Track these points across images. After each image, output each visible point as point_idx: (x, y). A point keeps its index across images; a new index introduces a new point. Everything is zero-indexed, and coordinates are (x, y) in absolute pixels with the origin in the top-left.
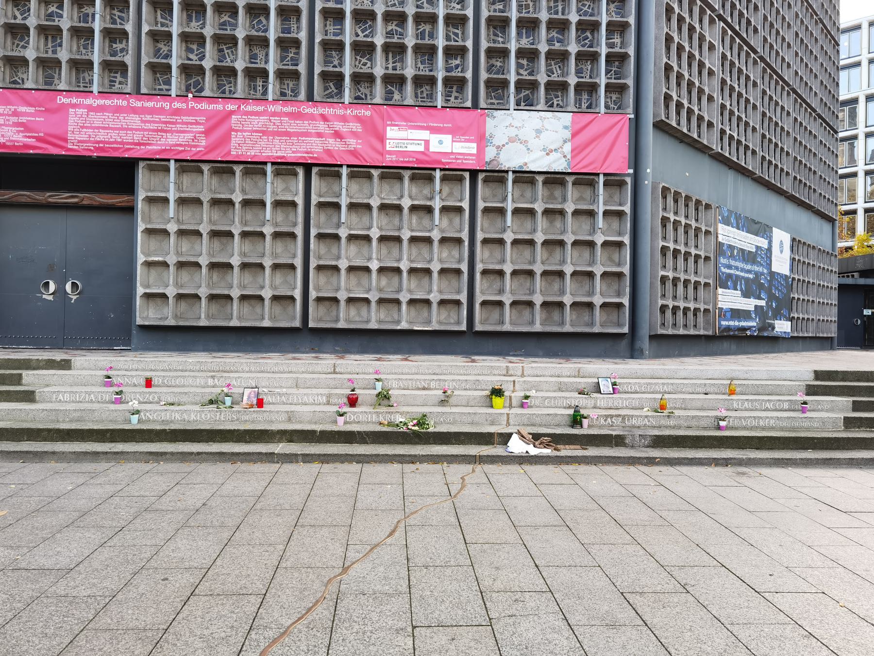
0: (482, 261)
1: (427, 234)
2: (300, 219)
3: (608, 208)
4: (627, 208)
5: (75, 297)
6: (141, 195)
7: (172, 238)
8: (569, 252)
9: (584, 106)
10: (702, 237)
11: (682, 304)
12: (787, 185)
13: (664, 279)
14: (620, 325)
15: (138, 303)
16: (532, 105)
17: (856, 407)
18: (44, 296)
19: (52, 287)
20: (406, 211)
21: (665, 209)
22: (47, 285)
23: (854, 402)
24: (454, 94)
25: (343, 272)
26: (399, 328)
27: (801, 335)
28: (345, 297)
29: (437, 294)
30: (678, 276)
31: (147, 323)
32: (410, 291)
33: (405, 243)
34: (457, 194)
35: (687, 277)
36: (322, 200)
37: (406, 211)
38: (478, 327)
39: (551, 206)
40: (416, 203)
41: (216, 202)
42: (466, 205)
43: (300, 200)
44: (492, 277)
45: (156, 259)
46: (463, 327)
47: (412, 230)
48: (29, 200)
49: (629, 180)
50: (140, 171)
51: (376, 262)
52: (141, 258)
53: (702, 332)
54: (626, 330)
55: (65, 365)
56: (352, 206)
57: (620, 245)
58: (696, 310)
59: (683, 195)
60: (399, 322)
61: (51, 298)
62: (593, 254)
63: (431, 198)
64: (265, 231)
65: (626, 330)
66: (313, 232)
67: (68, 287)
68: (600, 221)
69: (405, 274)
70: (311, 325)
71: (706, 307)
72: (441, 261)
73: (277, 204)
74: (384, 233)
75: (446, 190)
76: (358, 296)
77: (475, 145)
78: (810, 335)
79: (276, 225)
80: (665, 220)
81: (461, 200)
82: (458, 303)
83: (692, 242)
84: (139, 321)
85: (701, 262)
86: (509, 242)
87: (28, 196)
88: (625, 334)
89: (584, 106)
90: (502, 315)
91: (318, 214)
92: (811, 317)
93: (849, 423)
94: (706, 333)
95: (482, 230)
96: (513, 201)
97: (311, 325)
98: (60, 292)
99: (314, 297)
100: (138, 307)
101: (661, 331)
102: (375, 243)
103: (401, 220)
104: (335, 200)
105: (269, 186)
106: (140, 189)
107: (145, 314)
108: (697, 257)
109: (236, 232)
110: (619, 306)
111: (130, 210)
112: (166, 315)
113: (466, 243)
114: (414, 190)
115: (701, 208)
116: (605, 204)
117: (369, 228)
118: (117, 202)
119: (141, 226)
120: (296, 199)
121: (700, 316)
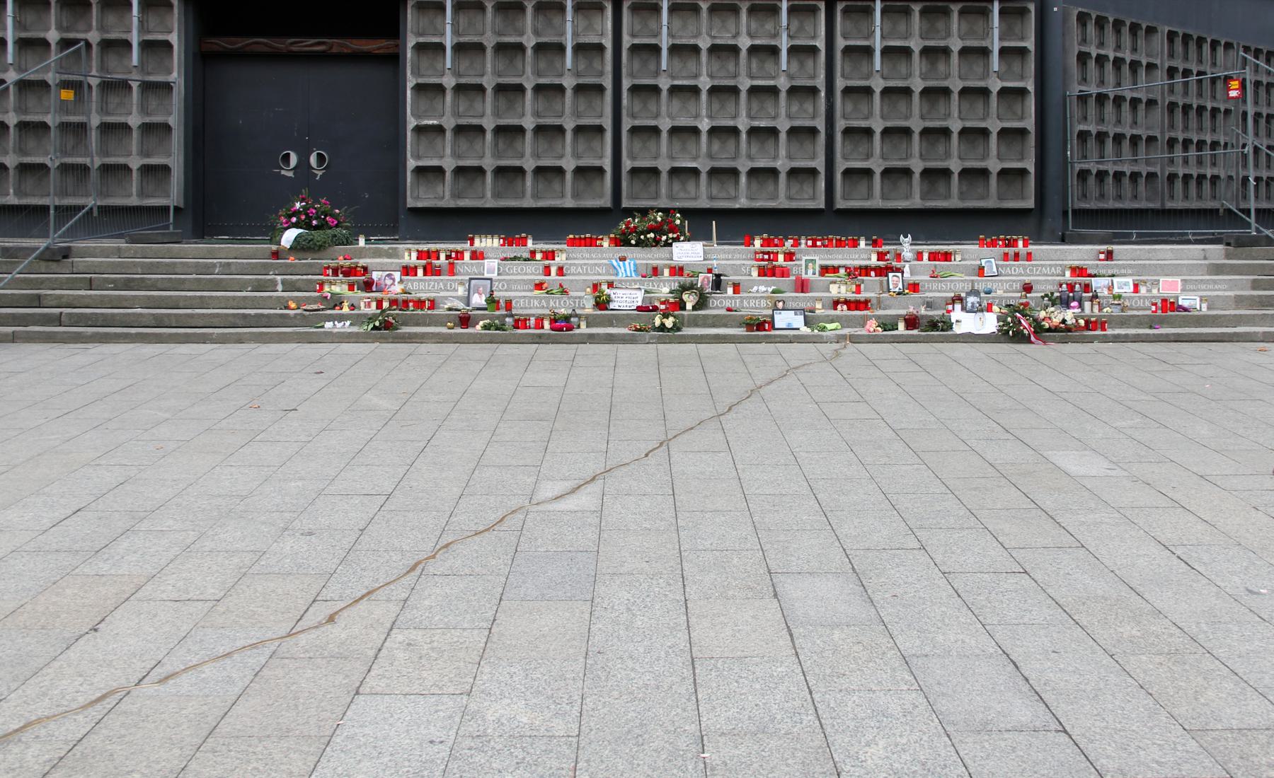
0: (844, 117)
1: (772, 83)
2: (609, 67)
3: (1006, 44)
4: (1030, 44)
5: (320, 173)
6: (411, 41)
7: (449, 97)
8: (957, 103)
14: (1023, 198)
15: (409, 180)
18: (283, 172)
20: (744, 53)
21: (1084, 41)
22: (286, 158)
25: (664, 135)
26: (737, 206)
28: (668, 168)
30: (1104, 129)
31: (420, 205)
32: (750, 157)
33: (743, 96)
36: (637, 41)
37: (744, 53)
38: (840, 204)
39: (932, 43)
40: (758, 42)
41: (501, 48)
42: (820, 43)
43: (608, 43)
45: (431, 122)
47: (752, 78)
48: (266, 49)
50: (409, 11)
51: (706, 120)
52: (412, 122)
54: (1030, 203)
56: (675, 49)
57: (1022, 92)
59: (1111, 20)
61: (290, 174)
63: (776, 35)
64: (565, 84)
65: (1030, 203)
66: (626, 84)
67: (313, 160)
69: (744, 136)
72: (789, 116)
73: (579, 48)
74: (716, 83)
75: (795, 24)
76: (684, 165)
79: (578, 75)
80: (1083, 57)
81: (814, 37)
84: (411, 203)
86: (878, 90)
87: (265, 44)
88: (1029, 210)
90: (870, 188)
91: (631, 59)
93: (1239, 301)
94: (1151, 205)
95: (843, 76)
96: (882, 37)
98: (303, 163)
100: (408, 184)
102: (704, 96)
103: (737, 64)
104: (653, 41)
105: (569, 26)
106: (409, 34)
109: (529, 86)
110: (1023, 172)
111: (394, 60)
112: (443, 196)
113: (823, 94)
114: (754, 25)
116: (1000, 39)
117: (696, 76)
118: (379, 49)
119: (411, 82)
120: (603, 41)
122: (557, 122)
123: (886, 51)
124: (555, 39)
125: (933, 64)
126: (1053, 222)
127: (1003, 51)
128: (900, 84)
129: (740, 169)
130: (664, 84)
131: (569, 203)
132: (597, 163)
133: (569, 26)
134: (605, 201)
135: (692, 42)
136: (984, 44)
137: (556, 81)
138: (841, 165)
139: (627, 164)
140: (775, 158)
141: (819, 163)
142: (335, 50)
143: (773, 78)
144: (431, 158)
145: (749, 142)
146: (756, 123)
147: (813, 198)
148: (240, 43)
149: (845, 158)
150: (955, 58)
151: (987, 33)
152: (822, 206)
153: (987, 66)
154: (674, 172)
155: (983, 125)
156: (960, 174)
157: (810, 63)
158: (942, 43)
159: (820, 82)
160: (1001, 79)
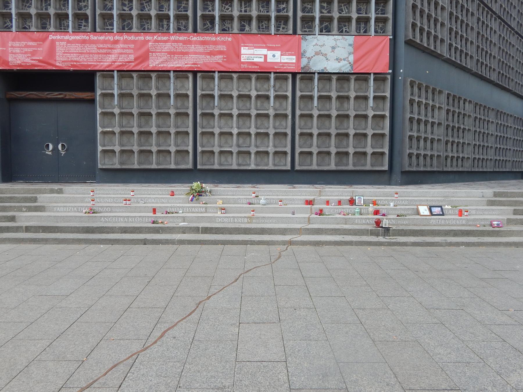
1: (266, 112)
2: (191, 104)
3: (376, 94)
4: (388, 94)
5: (63, 153)
6: (99, 92)
8: (353, 121)
9: (362, 31)
10: (436, 111)
11: (422, 153)
12: (494, 77)
13: (411, 138)
14: (382, 165)
15: (99, 156)
16: (330, 32)
17: (516, 212)
18: (47, 152)
19: (51, 147)
20: (253, 98)
21: (412, 94)
22: (48, 145)
23: (515, 210)
24: (282, 26)
26: (250, 168)
27: (501, 170)
29: (273, 148)
30: (420, 135)
31: (104, 167)
32: (256, 146)
33: (253, 118)
34: (284, 87)
35: (426, 136)
36: (204, 93)
37: (253, 98)
38: (297, 168)
39: (341, 94)
40: (260, 93)
42: (289, 94)
43: (190, 93)
44: (306, 137)
46: (289, 168)
47: (257, 110)
48: (35, 97)
49: (389, 77)
50: (97, 78)
51: (236, 129)
52: (100, 130)
53: (435, 169)
54: (386, 168)
55: (60, 191)
57: (383, 117)
58: (432, 157)
59: (424, 85)
60: (249, 165)
61: (50, 153)
62: (366, 122)
63: (268, 90)
64: (170, 112)
65: (386, 168)
66: (199, 112)
68: (371, 102)
69: (253, 136)
70: (199, 167)
71: (439, 154)
72: (275, 128)
74: (240, 112)
75: (278, 85)
76: (225, 149)
77: (294, 57)
78: (508, 170)
81: (286, 91)
82: (285, 153)
83: (430, 114)
84: (100, 166)
85: (436, 126)
87: (35, 95)
88: (386, 171)
89: (362, 31)
90: (312, 160)
91: (202, 101)
92: (508, 159)
95: (300, 109)
96: (318, 91)
97: (199, 167)
98: (55, 149)
99: (200, 151)
100: (99, 158)
101: (407, 169)
102: (235, 118)
105: (172, 85)
106: (98, 89)
107: (102, 163)
108: (433, 123)
109: (154, 113)
110: (383, 154)
111: (92, 101)
112: (115, 163)
113: (290, 117)
114: (259, 86)
115: (436, 93)
116: (374, 92)
117: (232, 109)
119: (99, 111)
120: (188, 93)
121: (435, 159)
122: (167, 129)
123: (320, 97)
124: (166, 92)
125: (342, 104)
126: (397, 176)
127: (375, 98)
128: (326, 113)
129: (251, 151)
130: (216, 112)
131: (173, 166)
132: (185, 148)
133: (172, 85)
134: (190, 166)
135: (229, 93)
136: (366, 94)
137: (167, 111)
138: (298, 150)
139: (199, 149)
140: (268, 146)
141: (288, 149)
142: (67, 97)
143: (268, 110)
144: (109, 147)
145: (256, 139)
146: (259, 131)
147: (285, 165)
148: (24, 94)
149: (300, 147)
150: (352, 101)
151: (367, 90)
152: (289, 168)
153: (367, 105)
154: (221, 152)
155: (365, 132)
156: (354, 154)
157: (284, 103)
158: (346, 94)
159: (289, 112)
160: (374, 111)
